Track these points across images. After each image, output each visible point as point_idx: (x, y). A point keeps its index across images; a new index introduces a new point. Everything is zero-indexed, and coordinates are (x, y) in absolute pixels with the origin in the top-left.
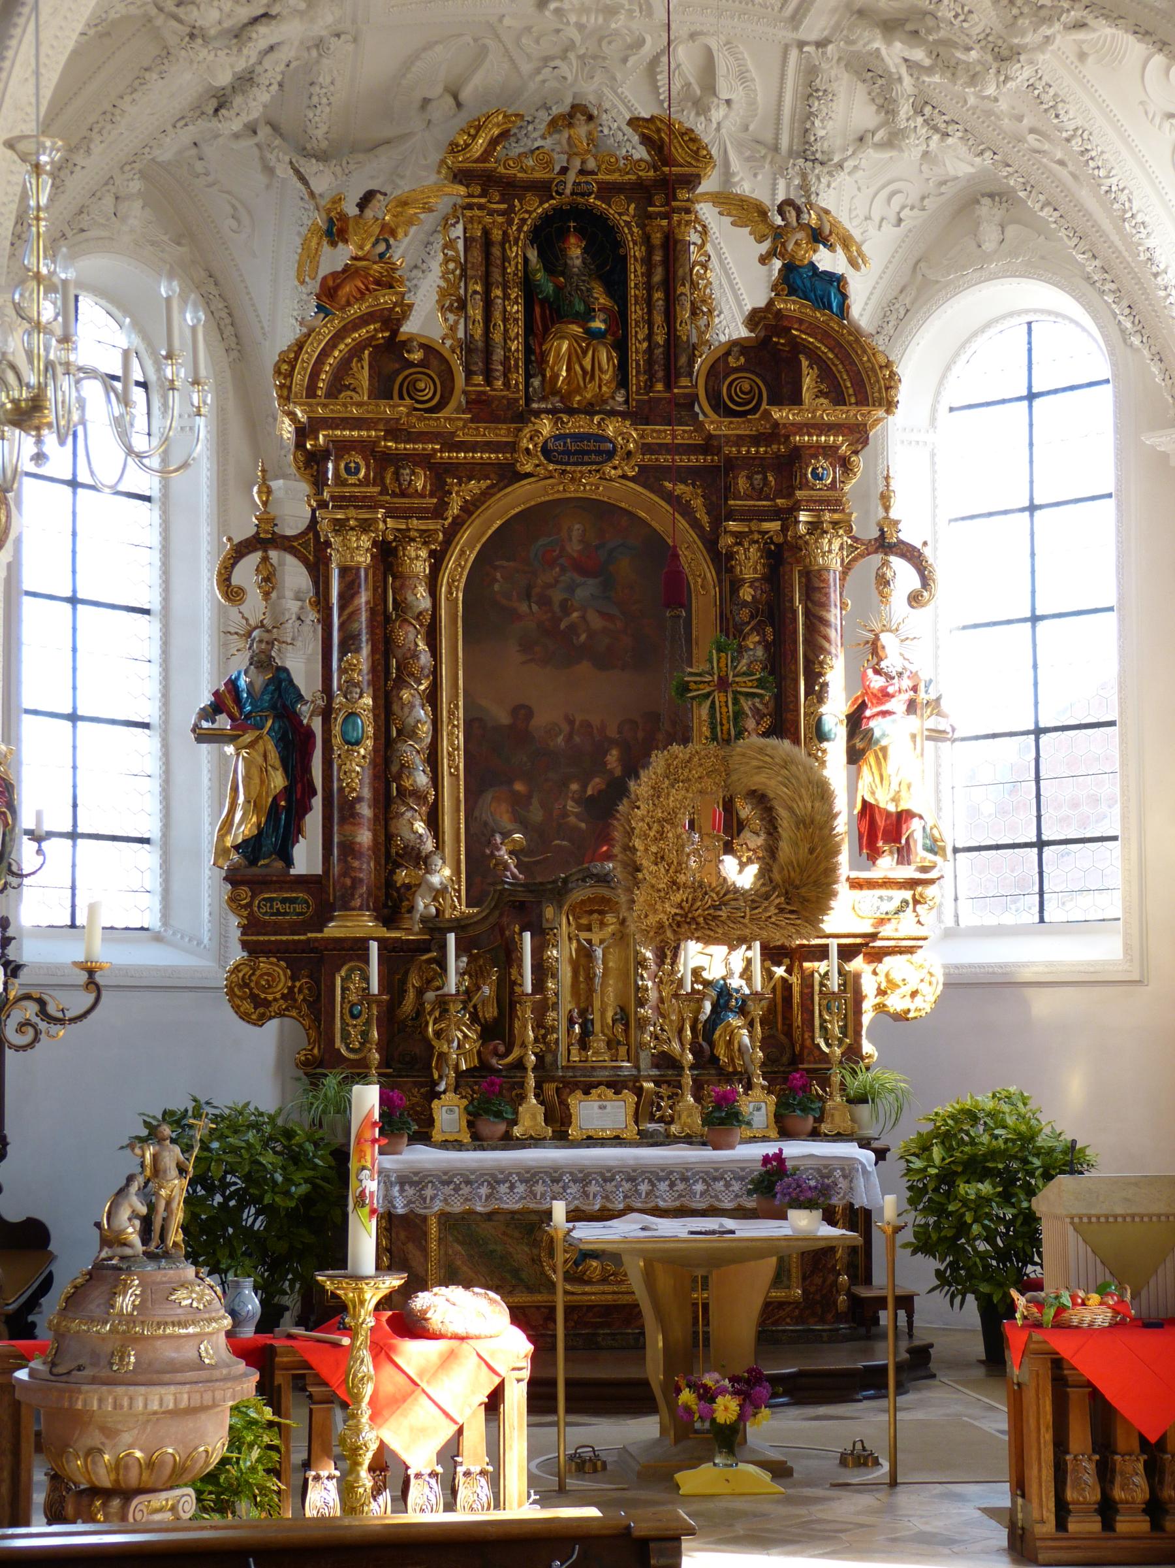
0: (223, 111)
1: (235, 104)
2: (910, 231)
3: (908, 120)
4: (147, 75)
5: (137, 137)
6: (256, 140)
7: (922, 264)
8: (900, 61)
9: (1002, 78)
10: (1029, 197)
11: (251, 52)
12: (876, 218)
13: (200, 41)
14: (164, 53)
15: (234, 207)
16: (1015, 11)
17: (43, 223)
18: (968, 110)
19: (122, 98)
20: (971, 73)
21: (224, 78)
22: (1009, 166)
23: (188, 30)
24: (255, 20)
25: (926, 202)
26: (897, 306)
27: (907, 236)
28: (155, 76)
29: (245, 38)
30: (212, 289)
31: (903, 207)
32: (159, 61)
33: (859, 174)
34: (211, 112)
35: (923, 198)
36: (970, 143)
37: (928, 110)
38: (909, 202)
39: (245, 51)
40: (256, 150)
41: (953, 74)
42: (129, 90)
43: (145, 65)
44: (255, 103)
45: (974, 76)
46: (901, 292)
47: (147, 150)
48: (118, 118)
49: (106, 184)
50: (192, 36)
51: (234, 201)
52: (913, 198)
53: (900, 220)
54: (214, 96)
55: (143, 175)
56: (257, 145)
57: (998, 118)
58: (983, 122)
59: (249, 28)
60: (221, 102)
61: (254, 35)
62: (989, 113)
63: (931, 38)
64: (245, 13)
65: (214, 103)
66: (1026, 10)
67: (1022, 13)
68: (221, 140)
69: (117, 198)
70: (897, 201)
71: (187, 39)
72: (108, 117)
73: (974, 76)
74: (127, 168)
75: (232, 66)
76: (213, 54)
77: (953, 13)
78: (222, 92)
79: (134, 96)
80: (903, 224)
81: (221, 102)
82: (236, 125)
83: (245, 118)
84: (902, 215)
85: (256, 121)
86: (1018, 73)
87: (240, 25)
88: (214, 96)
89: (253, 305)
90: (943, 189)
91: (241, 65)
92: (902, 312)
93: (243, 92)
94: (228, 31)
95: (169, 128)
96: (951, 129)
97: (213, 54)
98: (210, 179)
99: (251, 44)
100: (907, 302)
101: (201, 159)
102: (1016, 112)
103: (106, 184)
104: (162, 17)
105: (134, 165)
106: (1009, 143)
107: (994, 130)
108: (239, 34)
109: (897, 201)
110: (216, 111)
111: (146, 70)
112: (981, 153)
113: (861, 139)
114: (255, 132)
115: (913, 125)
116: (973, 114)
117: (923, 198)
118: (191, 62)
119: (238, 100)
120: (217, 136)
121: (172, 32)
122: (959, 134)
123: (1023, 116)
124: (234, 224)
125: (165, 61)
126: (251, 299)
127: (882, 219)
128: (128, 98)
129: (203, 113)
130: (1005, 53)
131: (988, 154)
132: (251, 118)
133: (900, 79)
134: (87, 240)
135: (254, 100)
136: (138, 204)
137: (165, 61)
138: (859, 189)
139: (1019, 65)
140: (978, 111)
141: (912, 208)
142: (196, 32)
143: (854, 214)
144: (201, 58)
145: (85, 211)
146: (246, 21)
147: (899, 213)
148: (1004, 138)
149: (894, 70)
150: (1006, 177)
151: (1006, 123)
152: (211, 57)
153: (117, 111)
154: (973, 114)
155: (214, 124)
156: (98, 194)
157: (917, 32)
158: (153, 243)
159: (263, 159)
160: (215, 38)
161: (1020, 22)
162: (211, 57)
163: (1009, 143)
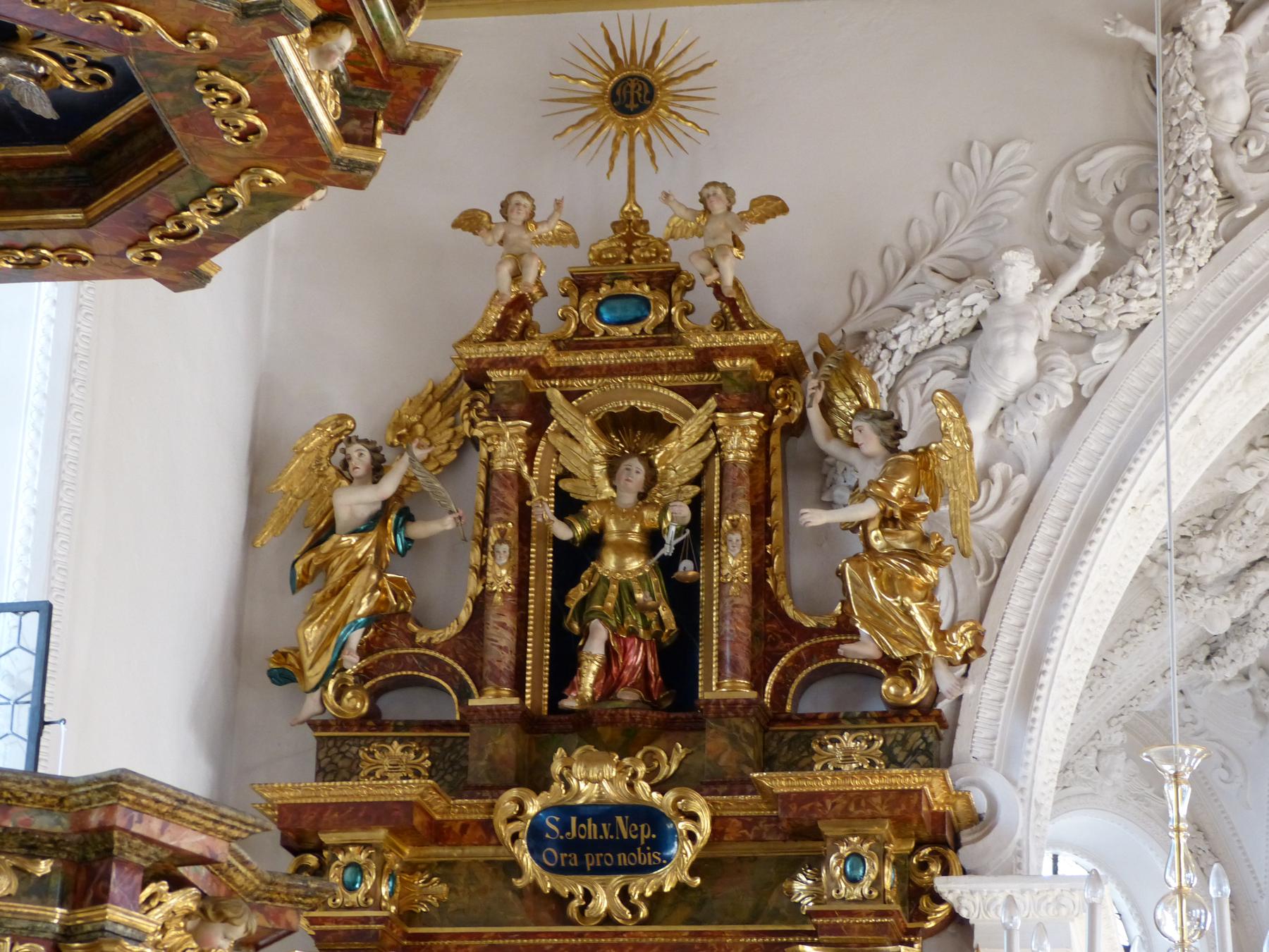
0: (1216, 659)
1: (1229, 651)
4: (1139, 627)
5: (1125, 689)
6: (1249, 685)
11: (1249, 596)
13: (1195, 590)
14: (1157, 604)
15: (1224, 757)
17: (1182, 834)
19: (1113, 651)
21: (1221, 626)
23: (1183, 579)
24: (1253, 565)
28: (1148, 627)
29: (1242, 581)
30: (1202, 844)
32: (1151, 612)
34: (1203, 659)
39: (1244, 597)
40: (1248, 696)
42: (1120, 643)
43: (1138, 616)
44: (1252, 649)
47: (1135, 701)
48: (1109, 672)
49: (1092, 739)
50: (1187, 585)
51: (1224, 750)
54: (1205, 643)
55: (1126, 728)
56: (1251, 691)
59: (1247, 574)
60: (1214, 650)
61: (1253, 581)
64: (1243, 559)
65: (1206, 651)
68: (1210, 688)
69: (1099, 751)
71: (1183, 588)
72: (1098, 672)
74: (1115, 721)
75: (1230, 614)
76: (1210, 601)
78: (1214, 639)
79: (1125, 649)
81: (1214, 650)
82: (1231, 672)
83: (1240, 665)
85: (1248, 668)
87: (1236, 571)
88: (1205, 643)
89: (1247, 860)
91: (1240, 611)
93: (1238, 638)
94: (1224, 577)
95: (1158, 678)
97: (1210, 601)
98: (1197, 728)
99: (1250, 590)
101: (1187, 707)
103: (1092, 739)
104: (1156, 567)
105: (1121, 718)
108: (1236, 580)
110: (1208, 658)
111: (1138, 622)
114: (1247, 677)
118: (1187, 612)
119: (1233, 647)
120: (1205, 684)
121: (1169, 582)
124: (1225, 775)
125: (1158, 612)
126: (1244, 854)
128: (1118, 651)
129: (1194, 661)
132: (1246, 664)
134: (1068, 797)
135: (1250, 645)
136: (1122, 757)
137: (1158, 612)
142: (1190, 580)
144: (1197, 607)
145: (1070, 767)
146: (1243, 567)
152: (1208, 605)
153: (1107, 665)
155: (1206, 672)
156: (1084, 750)
158: (1137, 798)
159: (1255, 705)
160: (1211, 586)
162: (1208, 605)
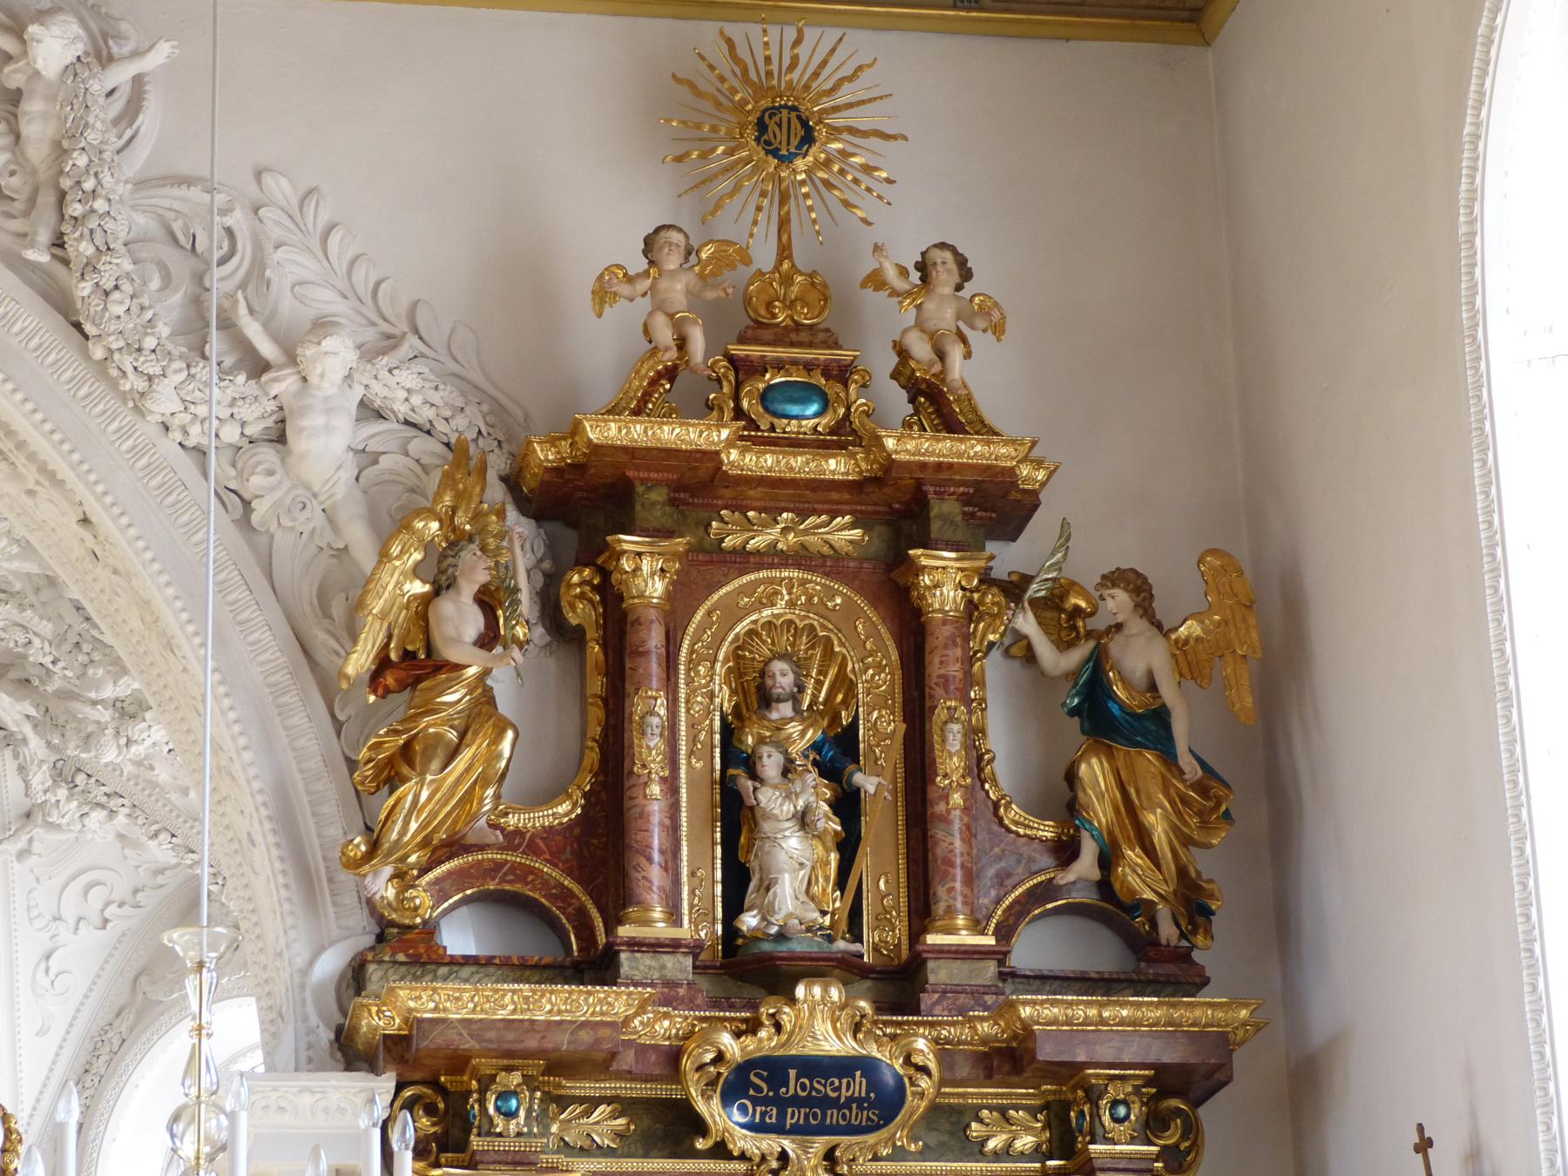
2: (124, 934)
3: (45, 792)
7: (143, 979)
8: (18, 717)
9: (123, 741)
10: (222, 892)
12: (69, 915)
16: (82, 658)
18: (129, 780)
20: (83, 734)
22: (193, 852)
25: (140, 896)
26: (110, 1035)
27: (120, 942)
31: (108, 904)
33: (32, 861)
35: (136, 891)
36: (141, 821)
37: (80, 779)
38: (116, 896)
41: (63, 736)
45: (88, 736)
46: (118, 1015)
52: (121, 890)
53: (106, 921)
57: (163, 790)
58: (150, 795)
62: (153, 784)
63: (49, 689)
66: (97, 656)
67: (92, 661)
70: (97, 896)
73: (88, 736)
77: (51, 658)
80: (109, 926)
84: (107, 914)
86: (144, 735)
90: (160, 880)
92: (116, 1043)
96: (114, 803)
100: (123, 1029)
102: (179, 782)
106: (185, 822)
107: (165, 805)
109: (97, 896)
112: (156, 835)
113: (28, 815)
115: (53, 800)
116: (137, 784)
117: (136, 891)
122: (126, 811)
123: (188, 789)
127: (80, 919)
130: (131, 709)
131: (164, 836)
133: (25, 741)
138: (38, 880)
139: (145, 725)
140: (140, 781)
141: (121, 905)
143: (35, 913)
147: (103, 911)
148: (178, 816)
149: (14, 729)
150: (191, 867)
151: (174, 797)
154: (137, 784)
157: (28, 681)
161: (91, 671)
163: (185, 822)
